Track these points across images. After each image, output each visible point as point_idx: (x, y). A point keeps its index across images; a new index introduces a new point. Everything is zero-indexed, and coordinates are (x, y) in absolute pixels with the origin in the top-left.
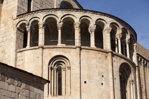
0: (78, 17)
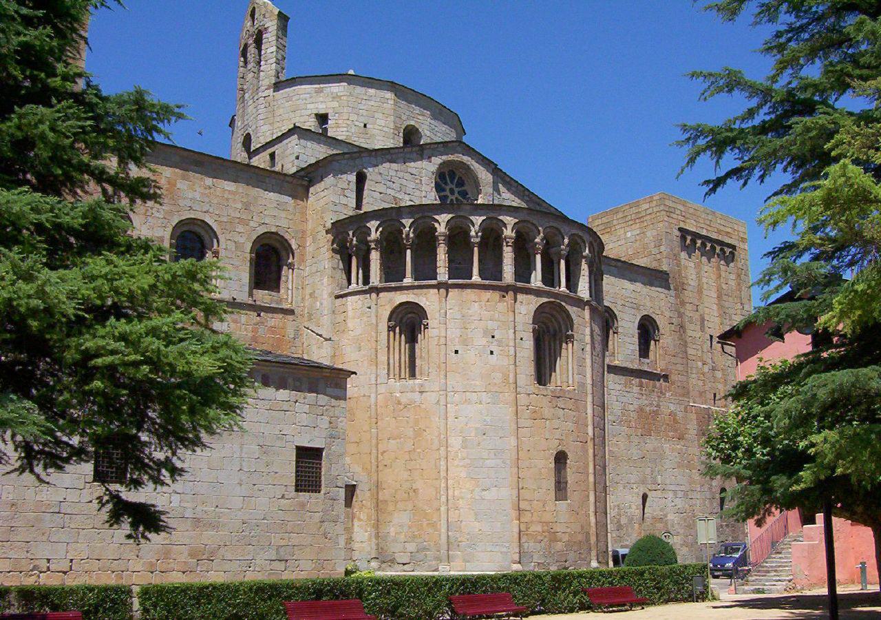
0: (444, 222)
